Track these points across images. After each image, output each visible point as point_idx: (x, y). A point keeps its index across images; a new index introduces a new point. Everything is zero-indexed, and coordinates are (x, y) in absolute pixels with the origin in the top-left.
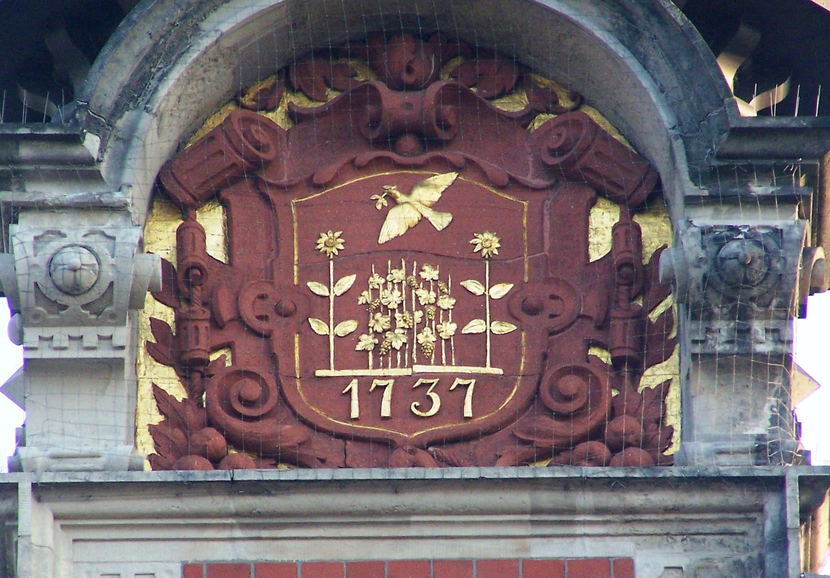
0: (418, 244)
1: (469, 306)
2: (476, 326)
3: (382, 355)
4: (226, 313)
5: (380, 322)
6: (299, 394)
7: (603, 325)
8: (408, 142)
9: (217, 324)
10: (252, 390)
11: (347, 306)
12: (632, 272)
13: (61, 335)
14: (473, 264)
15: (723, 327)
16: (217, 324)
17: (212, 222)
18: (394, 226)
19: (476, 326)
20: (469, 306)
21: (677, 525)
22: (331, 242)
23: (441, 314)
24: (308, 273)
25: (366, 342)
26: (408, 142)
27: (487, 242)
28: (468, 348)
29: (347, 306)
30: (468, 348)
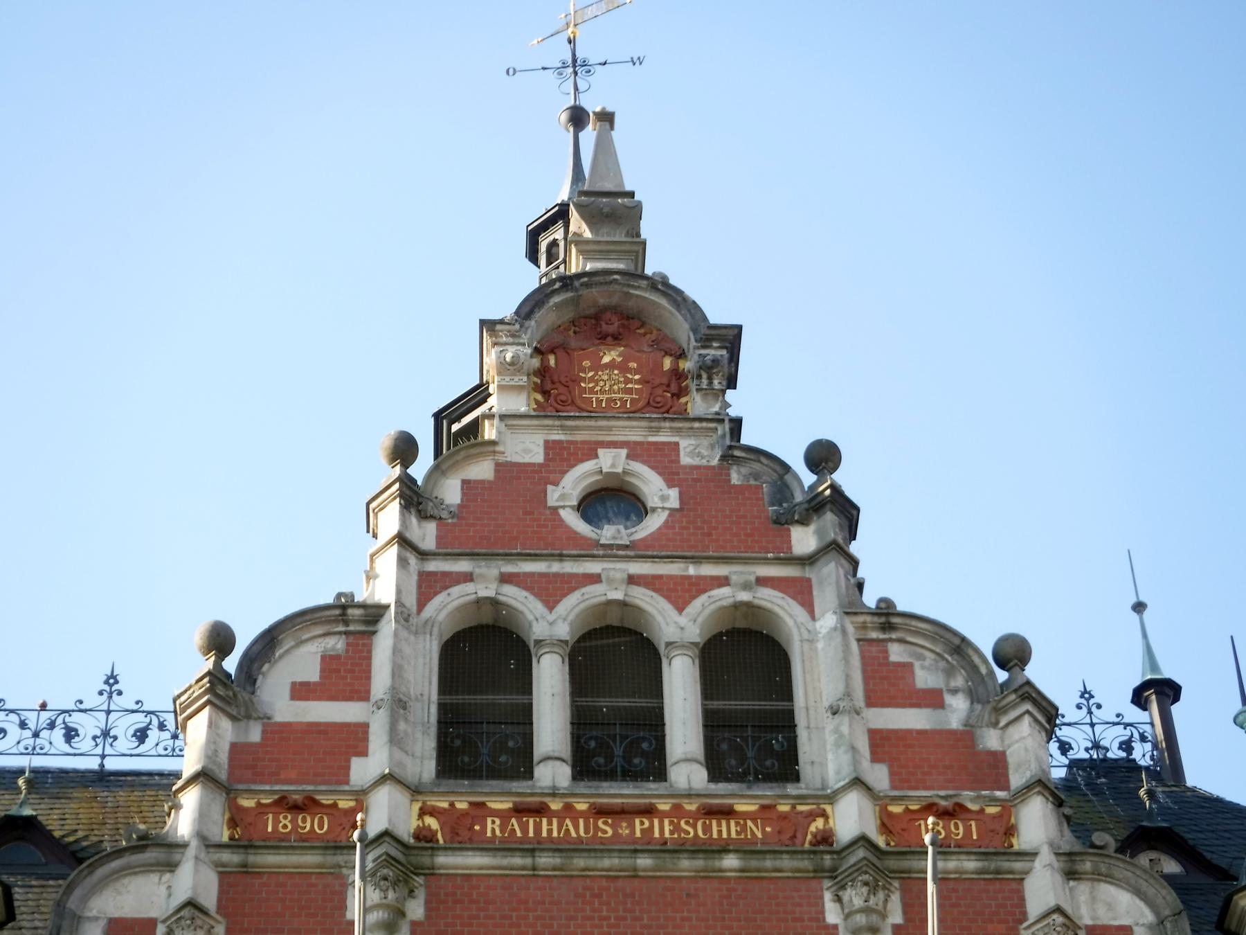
0: (612, 365)
1: (628, 381)
2: (630, 386)
3: (602, 392)
4: (556, 379)
5: (602, 383)
6: (578, 402)
7: (668, 386)
8: (609, 339)
9: (553, 383)
10: (563, 398)
11: (591, 379)
12: (678, 375)
13: (507, 379)
14: (629, 370)
15: (705, 381)
16: (553, 383)
17: (552, 361)
18: (606, 359)
19: (630, 386)
20: (628, 381)
21: (691, 432)
22: (586, 363)
23: (619, 382)
24: (580, 371)
25: (598, 388)
26: (609, 339)
27: (633, 365)
28: (629, 391)
29: (591, 379)
30: (629, 391)
